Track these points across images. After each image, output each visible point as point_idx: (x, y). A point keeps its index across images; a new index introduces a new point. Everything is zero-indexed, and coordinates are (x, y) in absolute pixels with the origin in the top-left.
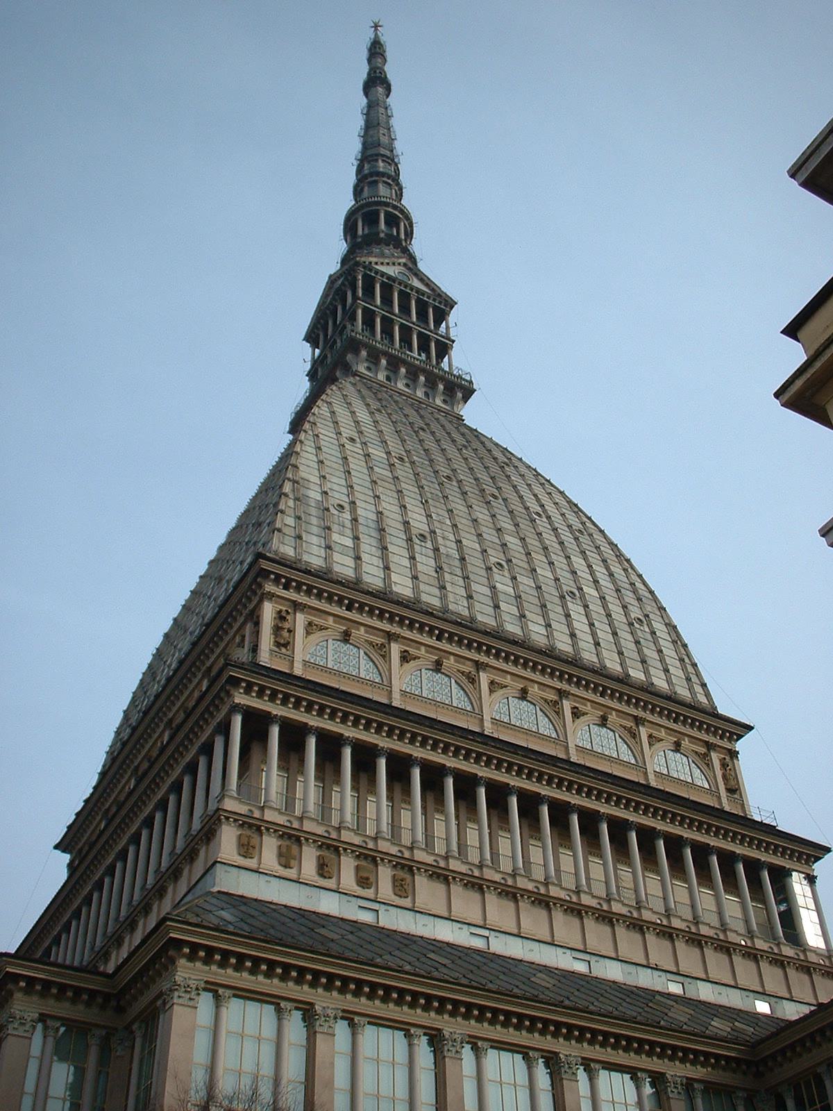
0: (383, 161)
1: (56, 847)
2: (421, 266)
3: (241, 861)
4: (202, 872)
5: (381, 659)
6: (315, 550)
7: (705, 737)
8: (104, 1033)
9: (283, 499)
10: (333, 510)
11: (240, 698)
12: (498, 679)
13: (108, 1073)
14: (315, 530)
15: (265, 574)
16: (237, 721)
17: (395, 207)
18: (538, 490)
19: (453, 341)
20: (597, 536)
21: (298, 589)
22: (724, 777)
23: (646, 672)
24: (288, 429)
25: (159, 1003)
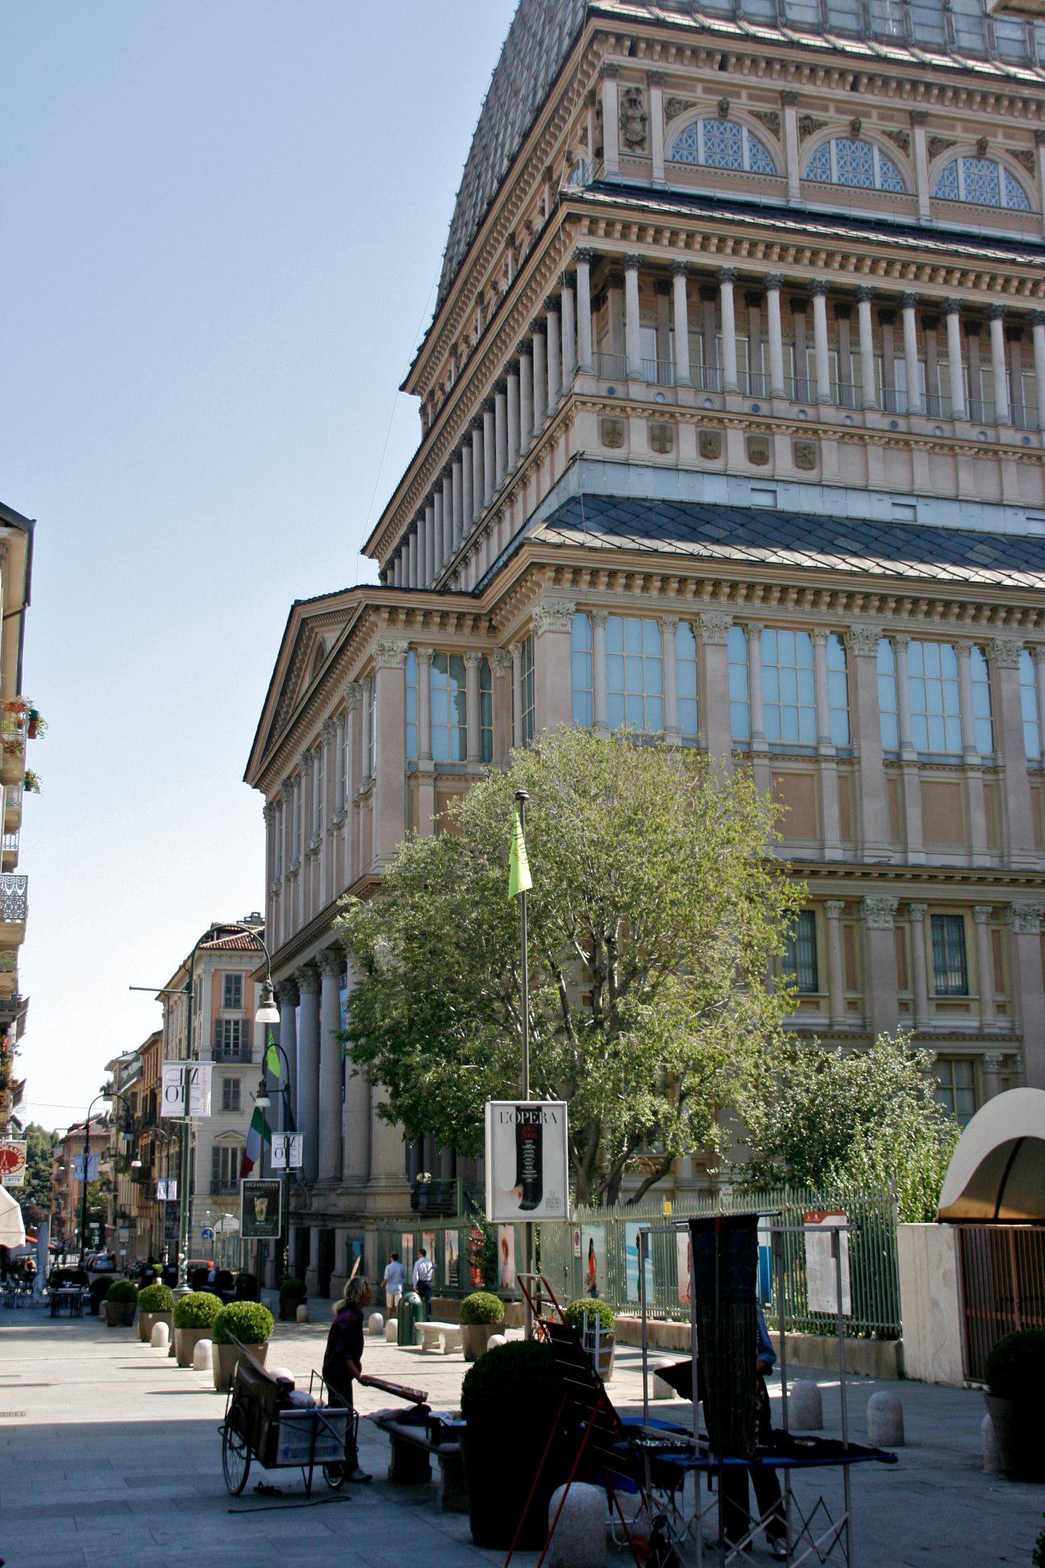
1: (402, 388)
8: (480, 655)
13: (490, 694)
16: (583, 272)
25: (531, 626)
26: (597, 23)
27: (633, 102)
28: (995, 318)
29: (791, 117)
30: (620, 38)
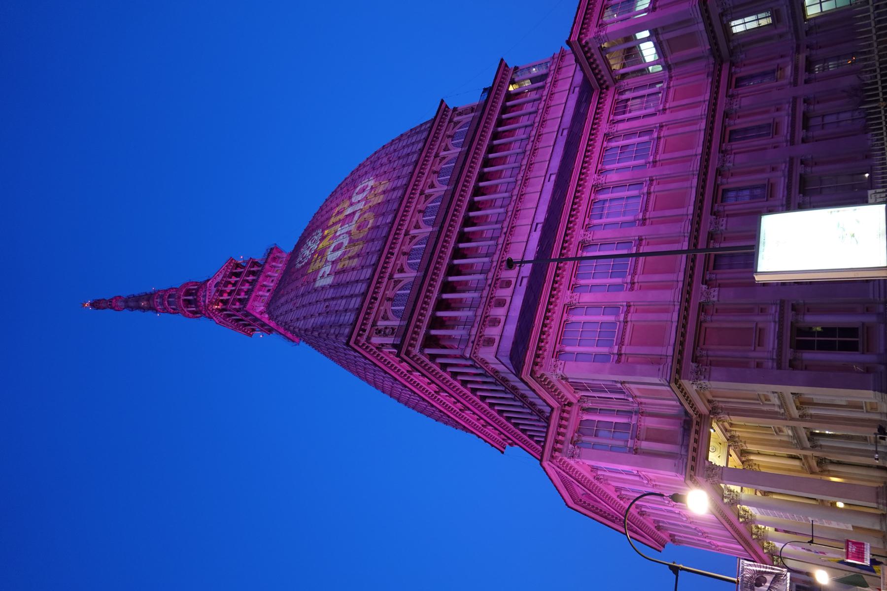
2: (211, 276)
3: (496, 344)
4: (503, 366)
5: (401, 283)
6: (347, 318)
7: (446, 124)
9: (321, 335)
10: (328, 310)
11: (416, 351)
12: (414, 224)
14: (337, 318)
15: (357, 342)
16: (428, 351)
18: (324, 212)
19: (251, 258)
20: (348, 181)
21: (365, 324)
22: (466, 114)
23: (414, 153)
26: (352, 343)
27: (380, 331)
28: (473, 199)
29: (397, 276)
30: (359, 335)
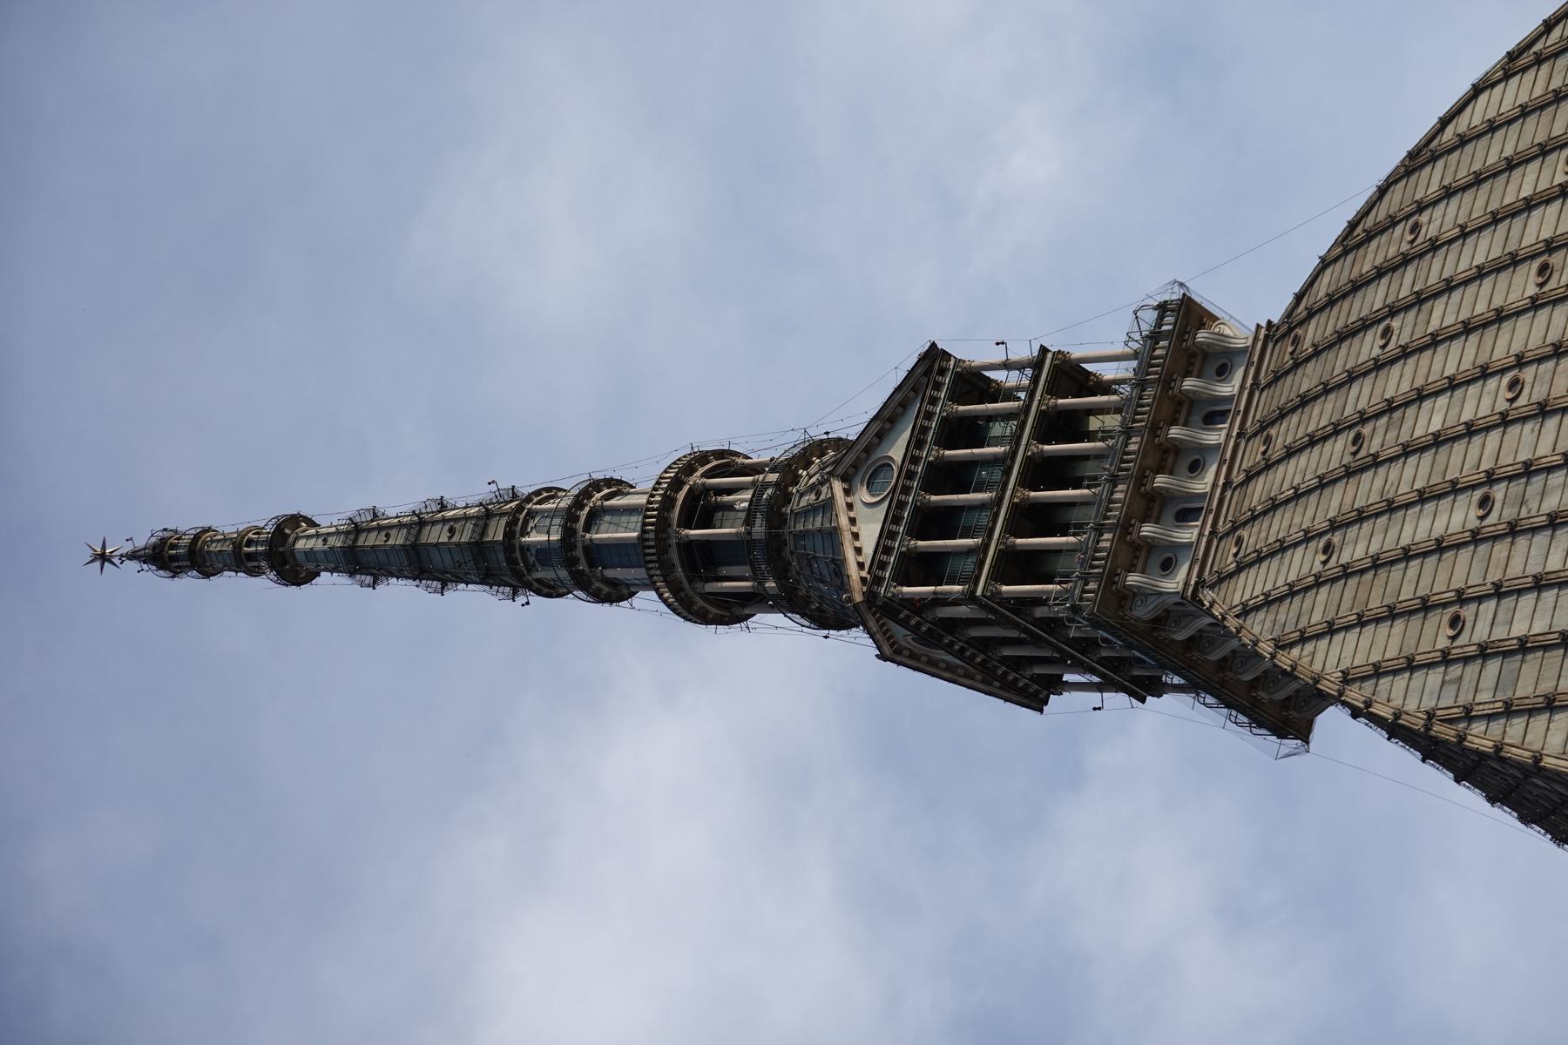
0: (524, 533)
17: (668, 502)
19: (1044, 350)
24: (1292, 744)
